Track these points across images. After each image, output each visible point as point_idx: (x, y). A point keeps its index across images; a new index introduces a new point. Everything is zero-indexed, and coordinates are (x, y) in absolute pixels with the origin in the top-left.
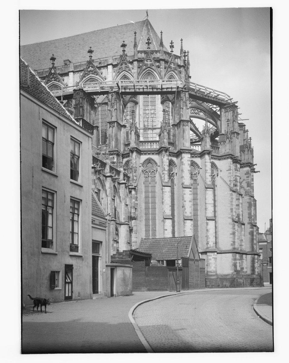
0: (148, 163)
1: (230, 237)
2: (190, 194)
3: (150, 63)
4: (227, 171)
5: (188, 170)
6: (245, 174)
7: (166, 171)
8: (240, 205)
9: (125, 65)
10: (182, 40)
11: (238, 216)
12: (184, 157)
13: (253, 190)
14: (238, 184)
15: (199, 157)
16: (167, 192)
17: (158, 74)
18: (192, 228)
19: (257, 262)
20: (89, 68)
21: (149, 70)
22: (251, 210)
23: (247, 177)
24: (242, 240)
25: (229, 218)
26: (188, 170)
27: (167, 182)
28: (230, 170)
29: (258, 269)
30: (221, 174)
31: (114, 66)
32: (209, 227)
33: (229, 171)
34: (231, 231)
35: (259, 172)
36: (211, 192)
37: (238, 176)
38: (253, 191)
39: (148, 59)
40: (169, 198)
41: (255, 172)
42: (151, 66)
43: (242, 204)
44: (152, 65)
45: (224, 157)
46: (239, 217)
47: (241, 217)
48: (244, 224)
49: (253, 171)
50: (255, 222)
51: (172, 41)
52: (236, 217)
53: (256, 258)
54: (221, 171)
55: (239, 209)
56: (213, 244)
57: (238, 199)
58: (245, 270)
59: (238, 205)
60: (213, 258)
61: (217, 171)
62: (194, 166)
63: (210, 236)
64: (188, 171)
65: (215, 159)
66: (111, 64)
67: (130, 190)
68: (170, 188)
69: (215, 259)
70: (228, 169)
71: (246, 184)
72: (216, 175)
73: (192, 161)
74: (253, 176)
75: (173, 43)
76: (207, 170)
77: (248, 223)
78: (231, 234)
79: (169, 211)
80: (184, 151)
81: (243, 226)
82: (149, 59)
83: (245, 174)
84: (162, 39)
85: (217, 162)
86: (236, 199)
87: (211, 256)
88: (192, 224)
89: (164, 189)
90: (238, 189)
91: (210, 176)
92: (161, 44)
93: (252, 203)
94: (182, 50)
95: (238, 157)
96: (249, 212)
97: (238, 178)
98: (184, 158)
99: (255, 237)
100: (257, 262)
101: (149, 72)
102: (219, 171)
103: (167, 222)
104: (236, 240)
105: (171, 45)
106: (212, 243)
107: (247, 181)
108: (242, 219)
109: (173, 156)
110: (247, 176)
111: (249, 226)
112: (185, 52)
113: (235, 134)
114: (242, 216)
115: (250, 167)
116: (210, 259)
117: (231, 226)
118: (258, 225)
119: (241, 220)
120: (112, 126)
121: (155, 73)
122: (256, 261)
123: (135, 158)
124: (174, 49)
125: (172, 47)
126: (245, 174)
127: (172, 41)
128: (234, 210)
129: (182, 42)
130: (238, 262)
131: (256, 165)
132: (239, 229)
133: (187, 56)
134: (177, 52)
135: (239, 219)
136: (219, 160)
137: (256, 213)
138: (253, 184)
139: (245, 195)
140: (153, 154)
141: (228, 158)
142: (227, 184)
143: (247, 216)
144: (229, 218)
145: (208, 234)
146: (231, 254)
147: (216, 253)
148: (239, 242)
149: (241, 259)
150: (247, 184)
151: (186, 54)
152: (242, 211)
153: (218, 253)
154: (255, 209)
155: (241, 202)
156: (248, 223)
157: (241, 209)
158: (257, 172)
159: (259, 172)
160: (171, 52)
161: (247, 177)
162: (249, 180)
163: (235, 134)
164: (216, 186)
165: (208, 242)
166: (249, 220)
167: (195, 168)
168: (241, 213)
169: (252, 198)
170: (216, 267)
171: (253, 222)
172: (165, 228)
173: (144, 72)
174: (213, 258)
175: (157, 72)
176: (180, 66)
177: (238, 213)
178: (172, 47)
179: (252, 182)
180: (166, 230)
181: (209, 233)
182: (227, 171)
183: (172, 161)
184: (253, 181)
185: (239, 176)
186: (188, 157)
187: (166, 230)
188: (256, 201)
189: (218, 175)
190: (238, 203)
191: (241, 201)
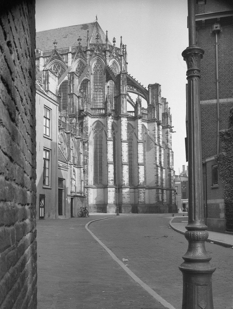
4: (153, 131)
6: (166, 133)
7: (110, 130)
10: (121, 37)
13: (171, 145)
16: (110, 145)
20: (54, 54)
22: (169, 158)
27: (110, 138)
31: (73, 54)
35: (175, 132)
38: (171, 146)
41: (172, 132)
49: (171, 131)
50: (173, 167)
51: (114, 38)
58: (165, 201)
66: (70, 53)
69: (144, 193)
74: (171, 135)
75: (115, 39)
78: (155, 176)
80: (123, 116)
84: (107, 36)
92: (107, 40)
94: (121, 44)
95: (160, 121)
99: (172, 178)
105: (113, 40)
110: (167, 134)
117: (155, 170)
118: (174, 169)
121: (102, 60)
124: (115, 43)
125: (114, 42)
126: (166, 133)
127: (114, 38)
129: (121, 39)
131: (173, 127)
133: (125, 48)
134: (118, 45)
137: (173, 161)
138: (171, 140)
147: (145, 189)
149: (162, 193)
151: (125, 47)
153: (146, 189)
158: (174, 132)
159: (175, 132)
160: (114, 45)
170: (144, 199)
171: (171, 167)
176: (121, 56)
178: (114, 42)
179: (171, 139)
182: (153, 131)
184: (171, 138)
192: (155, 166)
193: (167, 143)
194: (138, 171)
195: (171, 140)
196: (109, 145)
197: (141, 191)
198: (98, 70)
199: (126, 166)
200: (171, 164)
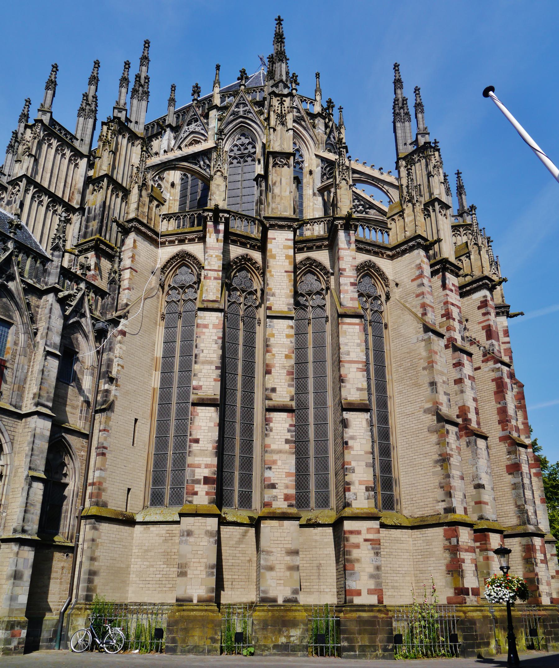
0: (179, 267)
1: (434, 474)
2: (288, 336)
3: (244, 109)
4: (413, 280)
5: (286, 272)
8: (467, 382)
9: (196, 124)
11: (463, 411)
12: (275, 239)
14: (456, 324)
15: (325, 246)
16: (211, 326)
17: (259, 127)
18: (292, 436)
19: (542, 561)
21: (242, 122)
22: (505, 399)
23: (484, 314)
24: (479, 486)
25: (426, 411)
26: (286, 272)
28: (421, 276)
29: (549, 584)
30: (396, 293)
32: (349, 433)
33: (419, 281)
34: (434, 453)
36: (357, 327)
37: (453, 304)
39: (241, 104)
40: (216, 343)
42: (245, 114)
43: (471, 378)
44: (248, 112)
45: (403, 248)
46: (466, 414)
47: (472, 416)
48: (485, 438)
52: (458, 417)
53: (538, 548)
54: (397, 285)
55: (462, 392)
56: (367, 489)
57: (458, 365)
59: (459, 381)
60: (366, 540)
61: (387, 286)
62: (314, 274)
63: (353, 464)
64: (285, 274)
65: (376, 254)
67: (100, 325)
68: (220, 315)
69: (376, 543)
70: (413, 277)
71: (484, 331)
72: (383, 298)
73: (308, 259)
76: (344, 270)
77: (502, 439)
78: (437, 462)
79: (213, 383)
81: (481, 443)
82: (243, 103)
83: (479, 308)
85: (383, 263)
86: (454, 364)
87: (358, 533)
88: (291, 425)
89: (201, 318)
90: (456, 337)
91: (352, 284)
93: (507, 380)
96: (499, 406)
97: (455, 312)
98: (273, 241)
100: (542, 561)
101: (242, 126)
102: (392, 284)
103: (200, 414)
104: (456, 483)
106: (363, 487)
107: (484, 324)
108: (478, 423)
109: (253, 247)
110: (483, 310)
111: (503, 448)
112: (330, 102)
113: (436, 204)
114: (477, 413)
115: (491, 289)
116: (357, 546)
117: (434, 438)
119: (474, 425)
120: (96, 188)
122: (539, 556)
123: (132, 245)
128: (441, 389)
130: (467, 557)
132: (467, 453)
135: (467, 420)
136: (392, 258)
137: (526, 418)
139: (483, 362)
140: (191, 241)
141: (412, 249)
142: (416, 315)
143: (496, 418)
144: (426, 411)
145: (347, 458)
146: (440, 531)
147: (375, 524)
148: (472, 491)
150: (486, 332)
152: (475, 400)
154: (521, 406)
155: (471, 375)
156: (502, 439)
157: (469, 395)
161: (484, 314)
162: (488, 320)
163: (436, 204)
164: (386, 326)
165: (348, 484)
166: (503, 430)
167: (318, 277)
168: (471, 405)
169: (505, 369)
172: (194, 437)
173: (231, 126)
174: (366, 540)
175: (258, 122)
177: (461, 404)
180: (197, 441)
181: (350, 453)
182: (413, 280)
183: (250, 260)
185: (458, 307)
186: (286, 240)
187: (197, 441)
188: (521, 386)
189: (388, 298)
190: (458, 376)
191: (468, 370)
192: (431, 419)
193: (490, 342)
194: (342, 438)
195: (509, 343)
196: (206, 326)
197: (358, 533)
198: (242, 154)
199: (286, 414)
200: (513, 422)
